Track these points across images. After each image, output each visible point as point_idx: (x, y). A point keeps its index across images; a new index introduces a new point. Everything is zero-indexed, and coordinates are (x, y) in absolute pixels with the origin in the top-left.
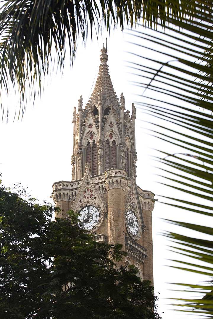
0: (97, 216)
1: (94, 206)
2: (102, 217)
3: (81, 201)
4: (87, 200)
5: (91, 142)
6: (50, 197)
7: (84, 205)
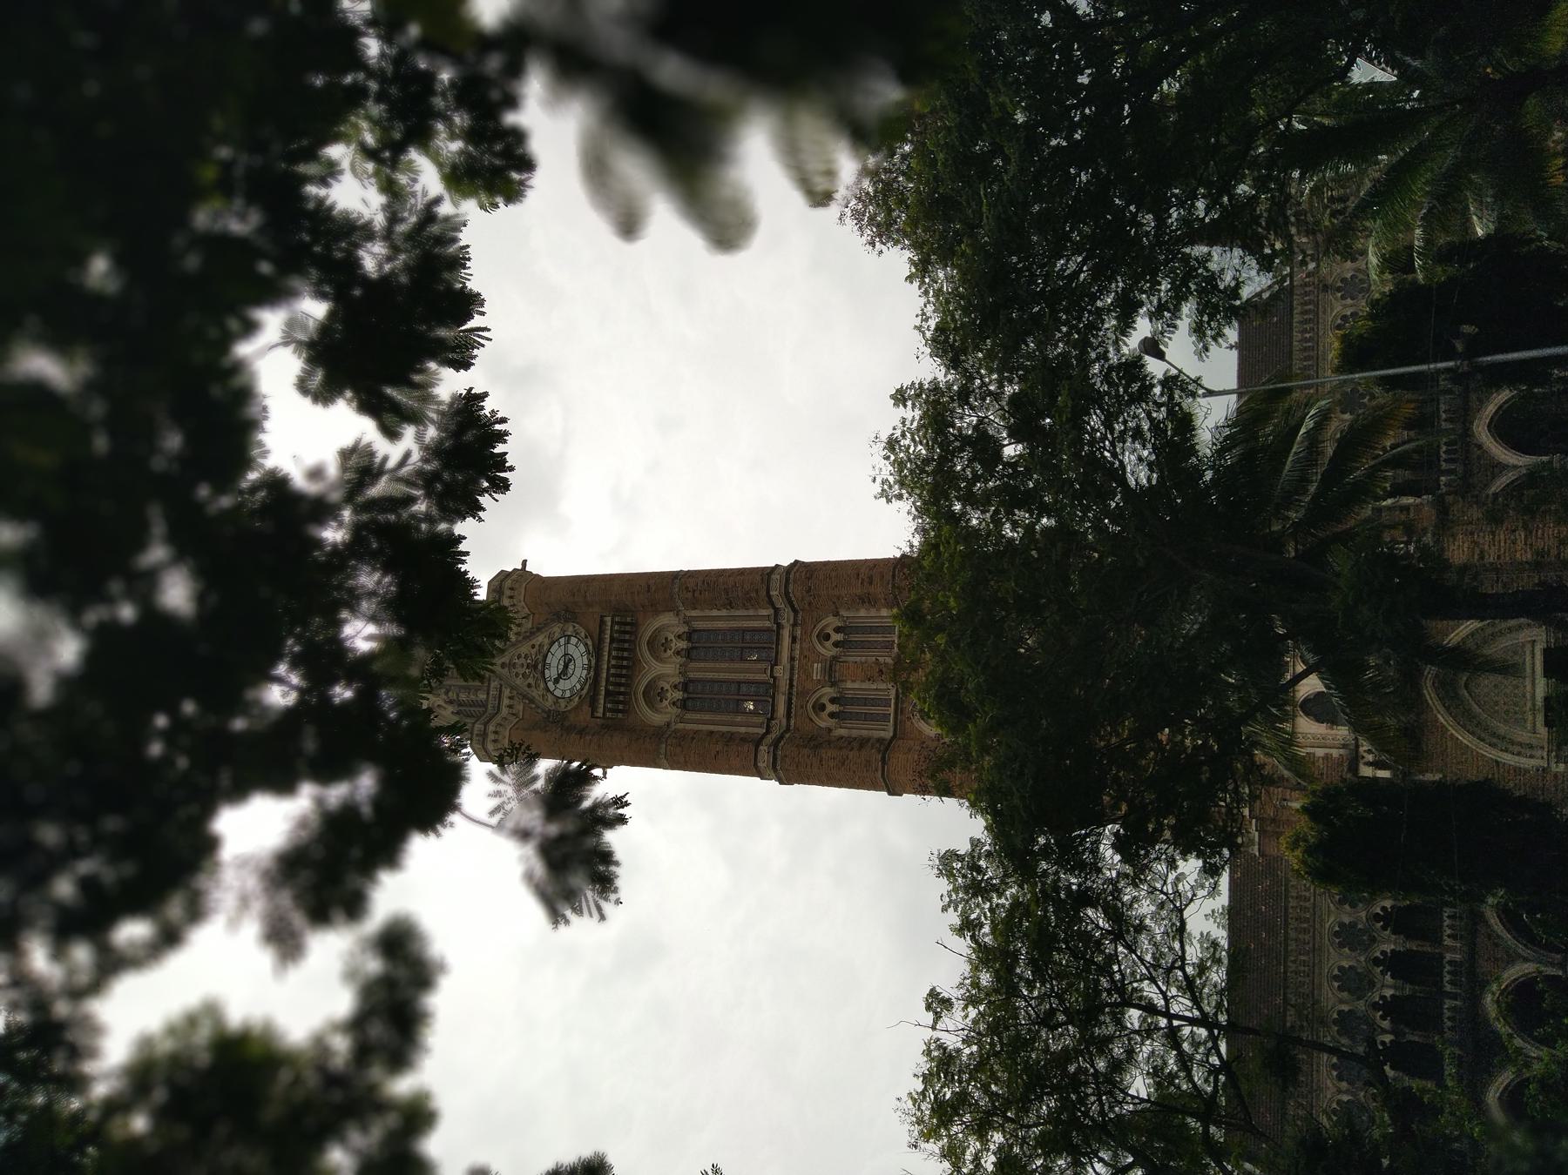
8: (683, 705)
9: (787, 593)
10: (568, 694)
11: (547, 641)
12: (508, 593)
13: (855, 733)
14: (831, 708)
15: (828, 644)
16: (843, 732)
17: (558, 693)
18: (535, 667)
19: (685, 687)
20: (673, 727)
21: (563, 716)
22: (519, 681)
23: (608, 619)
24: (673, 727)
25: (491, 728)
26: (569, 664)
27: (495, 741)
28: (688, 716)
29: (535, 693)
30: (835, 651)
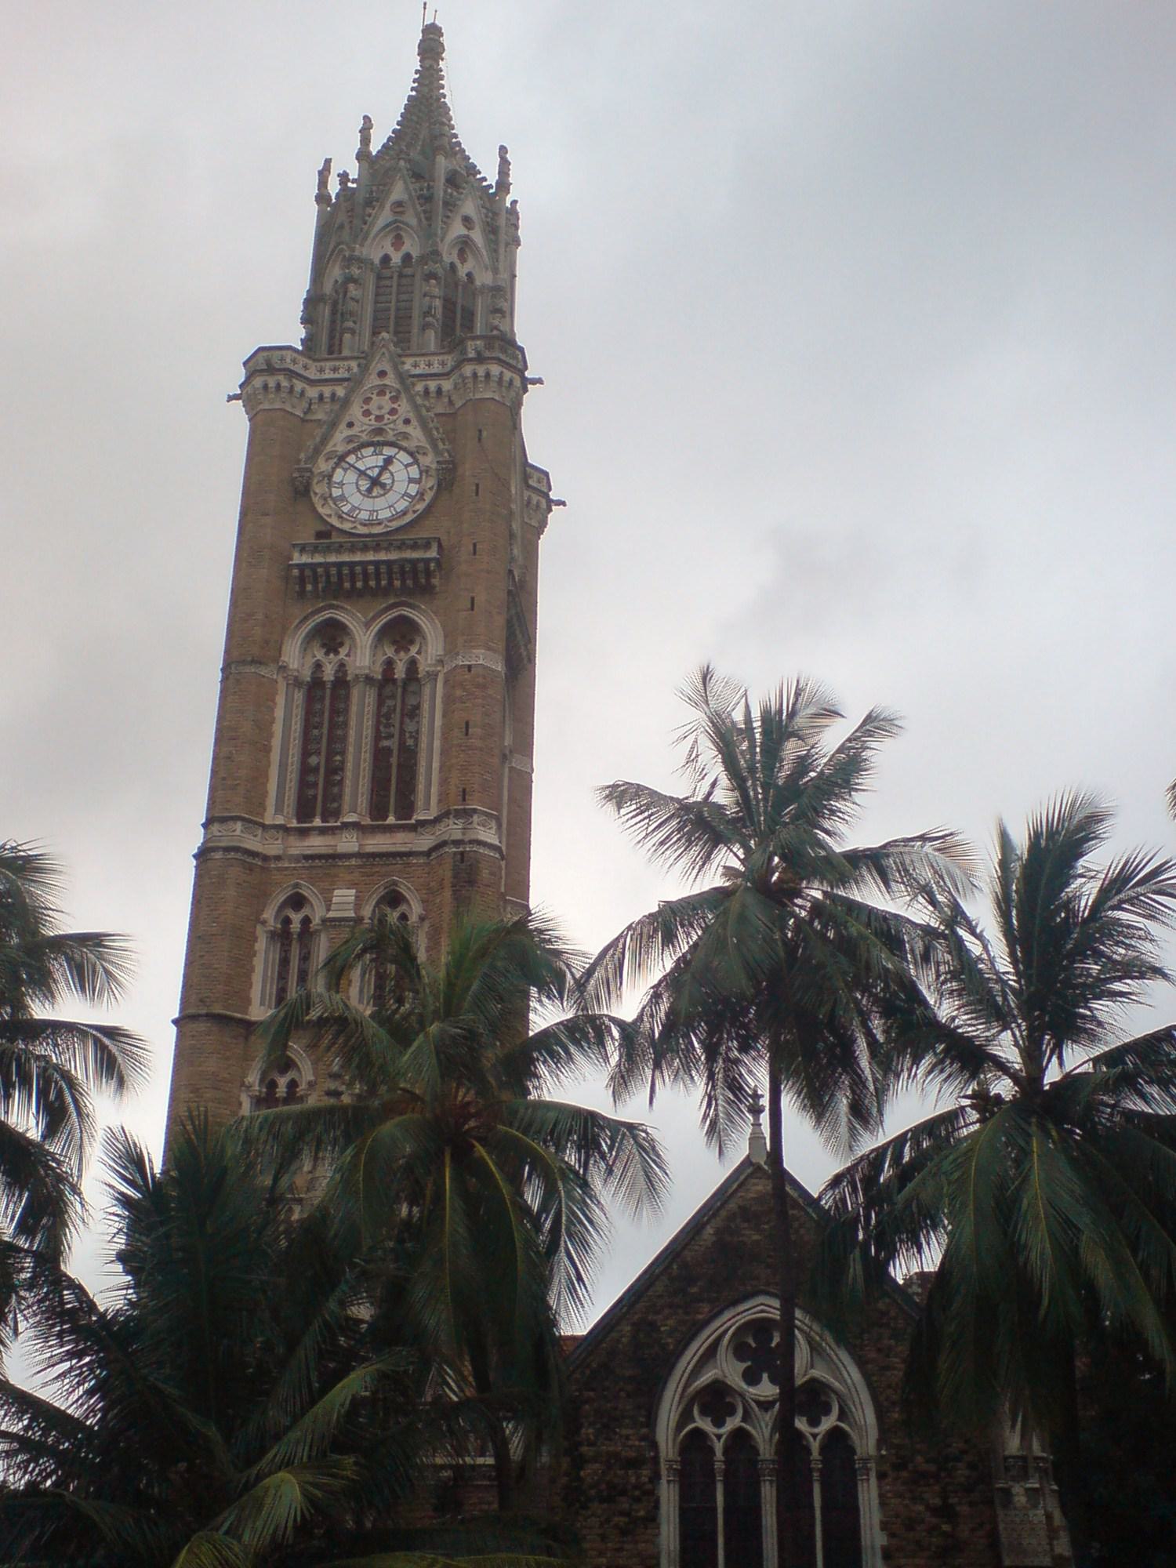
0: (411, 480)
1: (401, 448)
2: (431, 482)
3: (350, 425)
4: (377, 425)
5: (396, 259)
6: (230, 398)
7: (365, 437)
8: (314, 687)
9: (444, 844)
10: (336, 492)
11: (411, 445)
12: (481, 371)
14: (296, 918)
17: (338, 475)
19: (341, 683)
21: (301, 491)
23: (433, 553)
26: (376, 491)
27: (266, 387)
28: (299, 696)
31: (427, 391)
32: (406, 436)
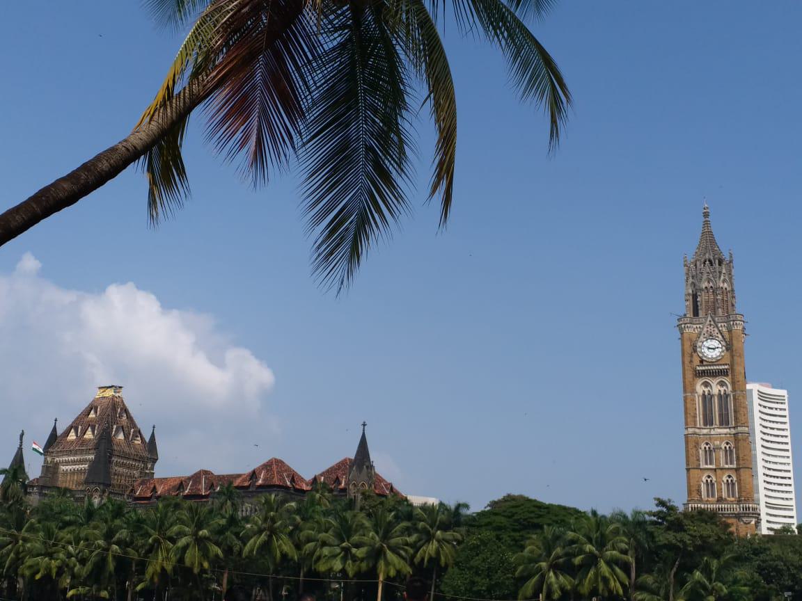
11: (720, 340)
13: (701, 456)
15: (725, 445)
16: (701, 452)
18: (711, 336)
20: (696, 395)
21: (695, 351)
22: (705, 329)
23: (726, 367)
24: (696, 395)
25: (689, 325)
28: (700, 398)
29: (701, 337)
30: (723, 448)
31: (721, 326)
32: (718, 337)
